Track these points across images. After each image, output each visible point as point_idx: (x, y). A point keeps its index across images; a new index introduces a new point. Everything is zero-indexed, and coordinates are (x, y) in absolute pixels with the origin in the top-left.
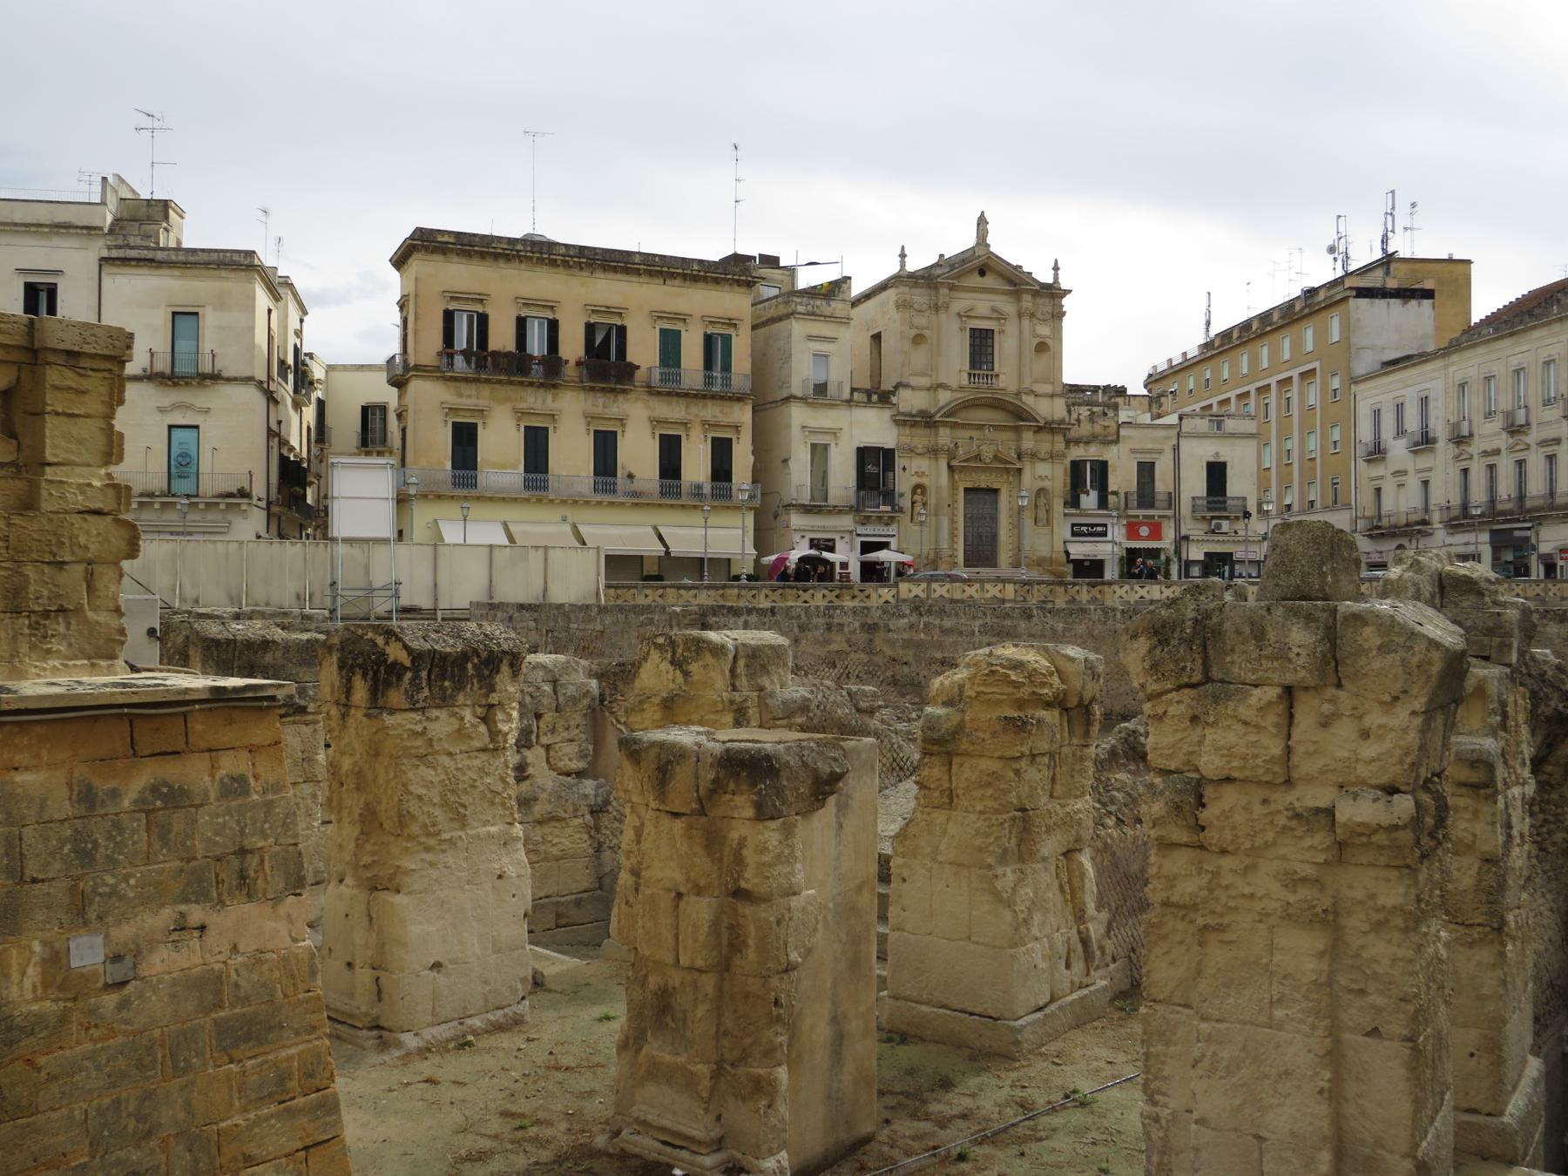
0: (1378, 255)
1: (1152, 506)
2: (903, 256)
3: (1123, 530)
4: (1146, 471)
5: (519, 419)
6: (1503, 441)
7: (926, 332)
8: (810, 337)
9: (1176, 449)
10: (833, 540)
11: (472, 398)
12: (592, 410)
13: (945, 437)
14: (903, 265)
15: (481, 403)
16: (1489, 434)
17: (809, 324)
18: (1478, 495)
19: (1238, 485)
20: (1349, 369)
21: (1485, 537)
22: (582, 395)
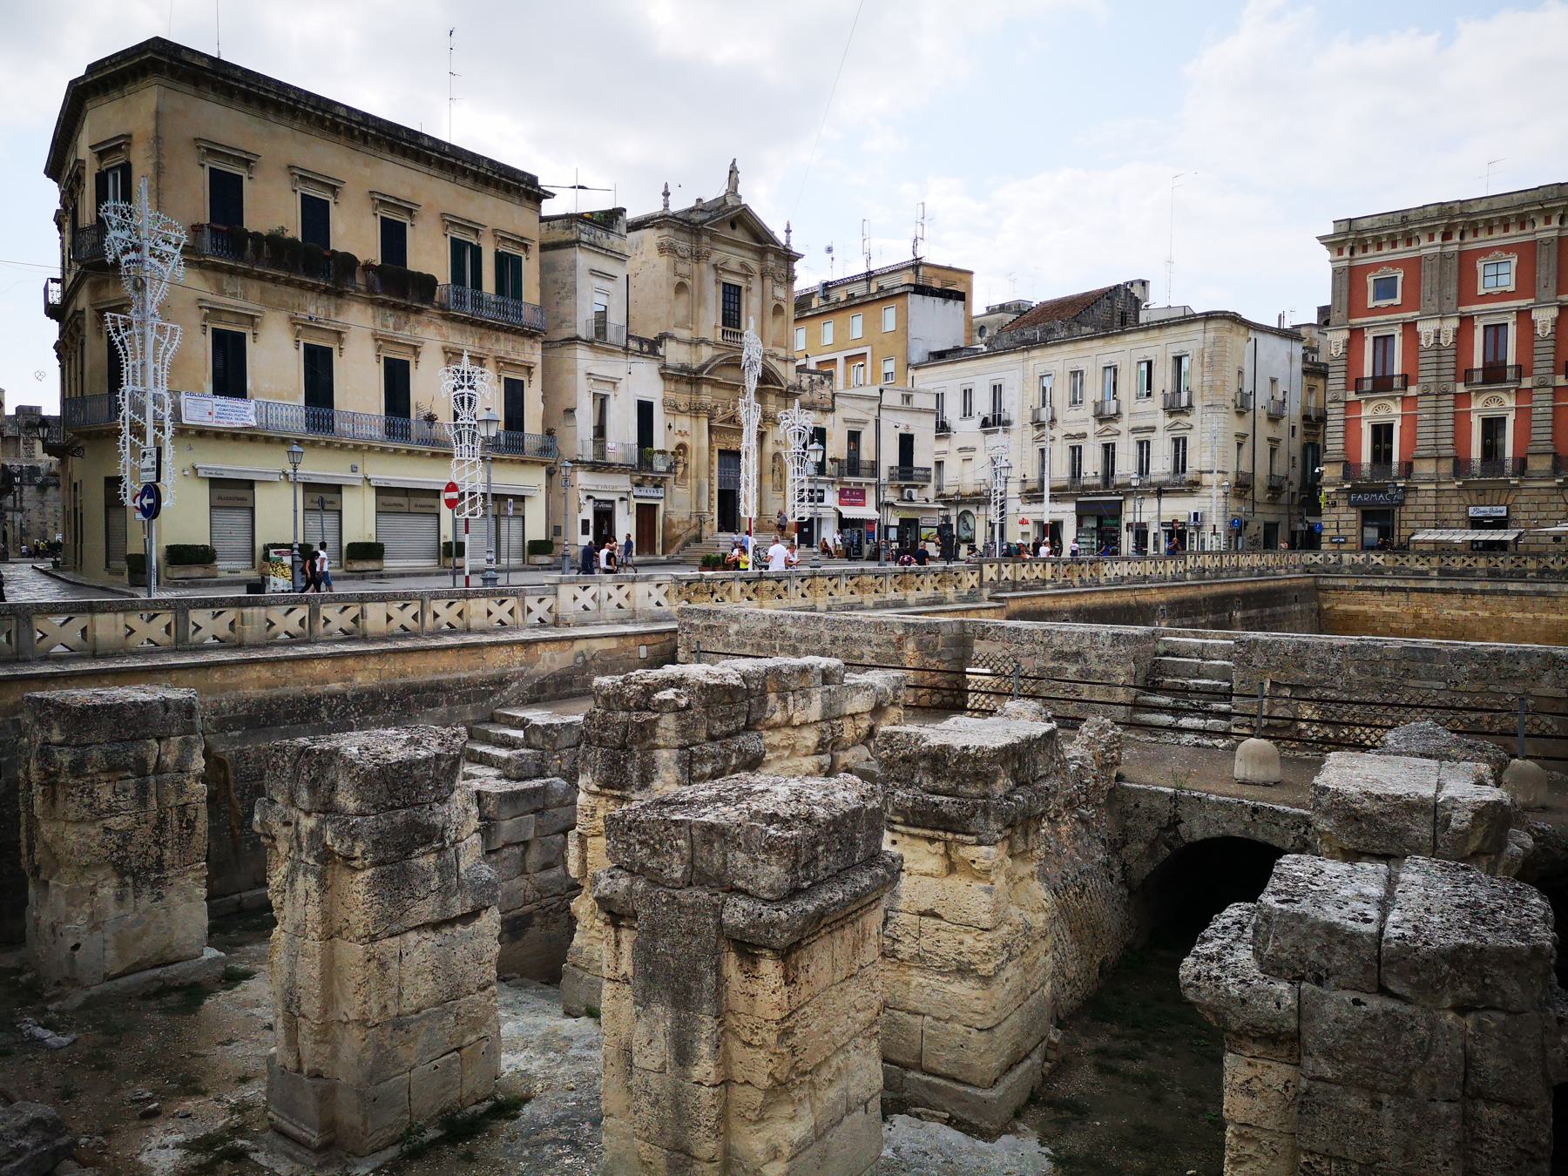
0: (908, 257)
1: (857, 474)
2: (666, 194)
3: (837, 496)
4: (854, 437)
5: (298, 334)
6: (1091, 427)
7: (688, 282)
8: (593, 272)
9: (878, 422)
10: (612, 502)
11: (241, 297)
12: (383, 331)
13: (707, 395)
14: (666, 206)
15: (249, 306)
16: (1080, 420)
17: (592, 256)
18: (1059, 471)
19: (922, 459)
20: (906, 356)
21: (1072, 507)
22: (370, 311)
